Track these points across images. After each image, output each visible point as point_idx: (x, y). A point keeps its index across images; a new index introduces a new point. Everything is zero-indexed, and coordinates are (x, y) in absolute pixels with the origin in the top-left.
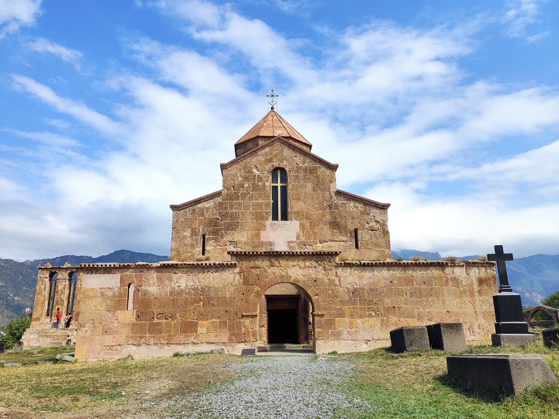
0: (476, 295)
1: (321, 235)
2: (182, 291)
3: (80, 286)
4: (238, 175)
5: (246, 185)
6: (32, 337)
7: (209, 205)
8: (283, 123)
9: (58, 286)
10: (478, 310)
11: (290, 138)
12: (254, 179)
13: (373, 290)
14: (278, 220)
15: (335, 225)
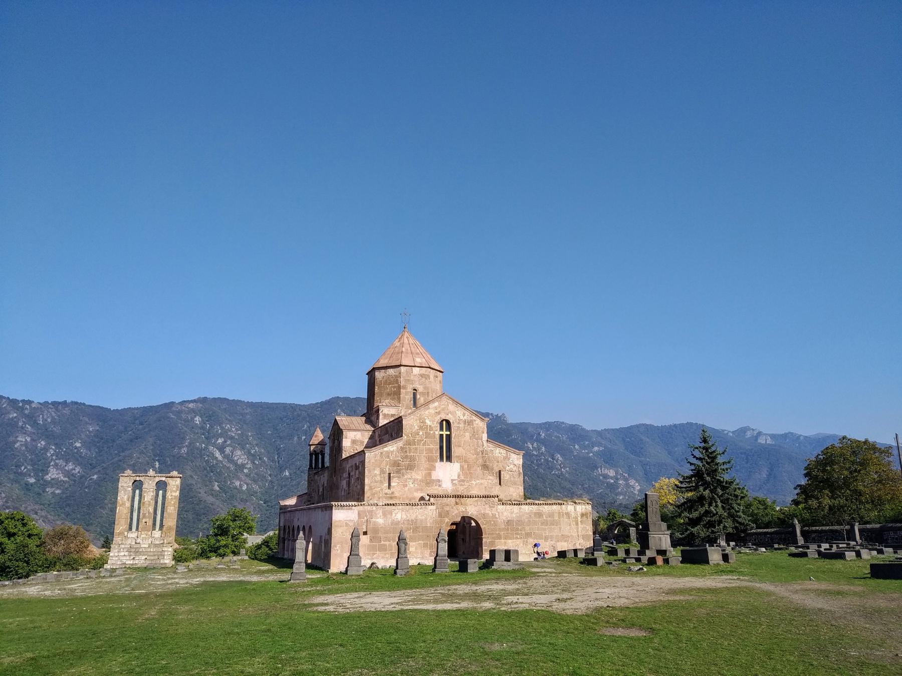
0: (580, 523)
1: (475, 474)
2: (399, 522)
3: (170, 497)
4: (415, 425)
5: (421, 433)
6: (122, 554)
7: (393, 449)
8: (418, 347)
9: (144, 497)
10: (580, 534)
11: (430, 368)
12: (427, 428)
13: (519, 522)
14: (443, 461)
15: (485, 467)
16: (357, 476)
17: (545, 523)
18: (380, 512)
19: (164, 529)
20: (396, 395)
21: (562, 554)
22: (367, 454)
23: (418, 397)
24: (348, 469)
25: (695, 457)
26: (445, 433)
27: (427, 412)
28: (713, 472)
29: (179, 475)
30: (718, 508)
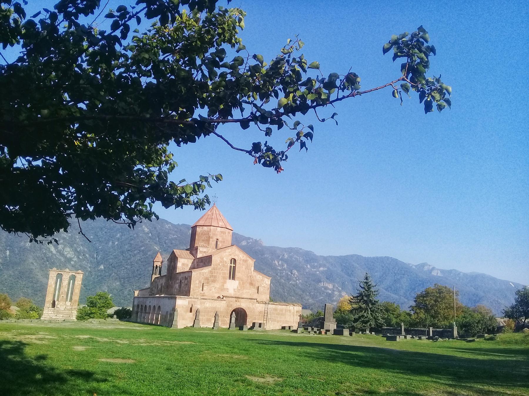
2: (207, 308)
5: (221, 264)
6: (50, 313)
15: (251, 284)
16: (186, 283)
17: (278, 314)
18: (199, 302)
19: (73, 301)
20: (208, 241)
21: (283, 328)
22: (193, 273)
23: (219, 243)
24: (180, 279)
25: (361, 286)
26: (232, 265)
27: (224, 254)
28: (368, 296)
29: (82, 273)
30: (368, 315)
